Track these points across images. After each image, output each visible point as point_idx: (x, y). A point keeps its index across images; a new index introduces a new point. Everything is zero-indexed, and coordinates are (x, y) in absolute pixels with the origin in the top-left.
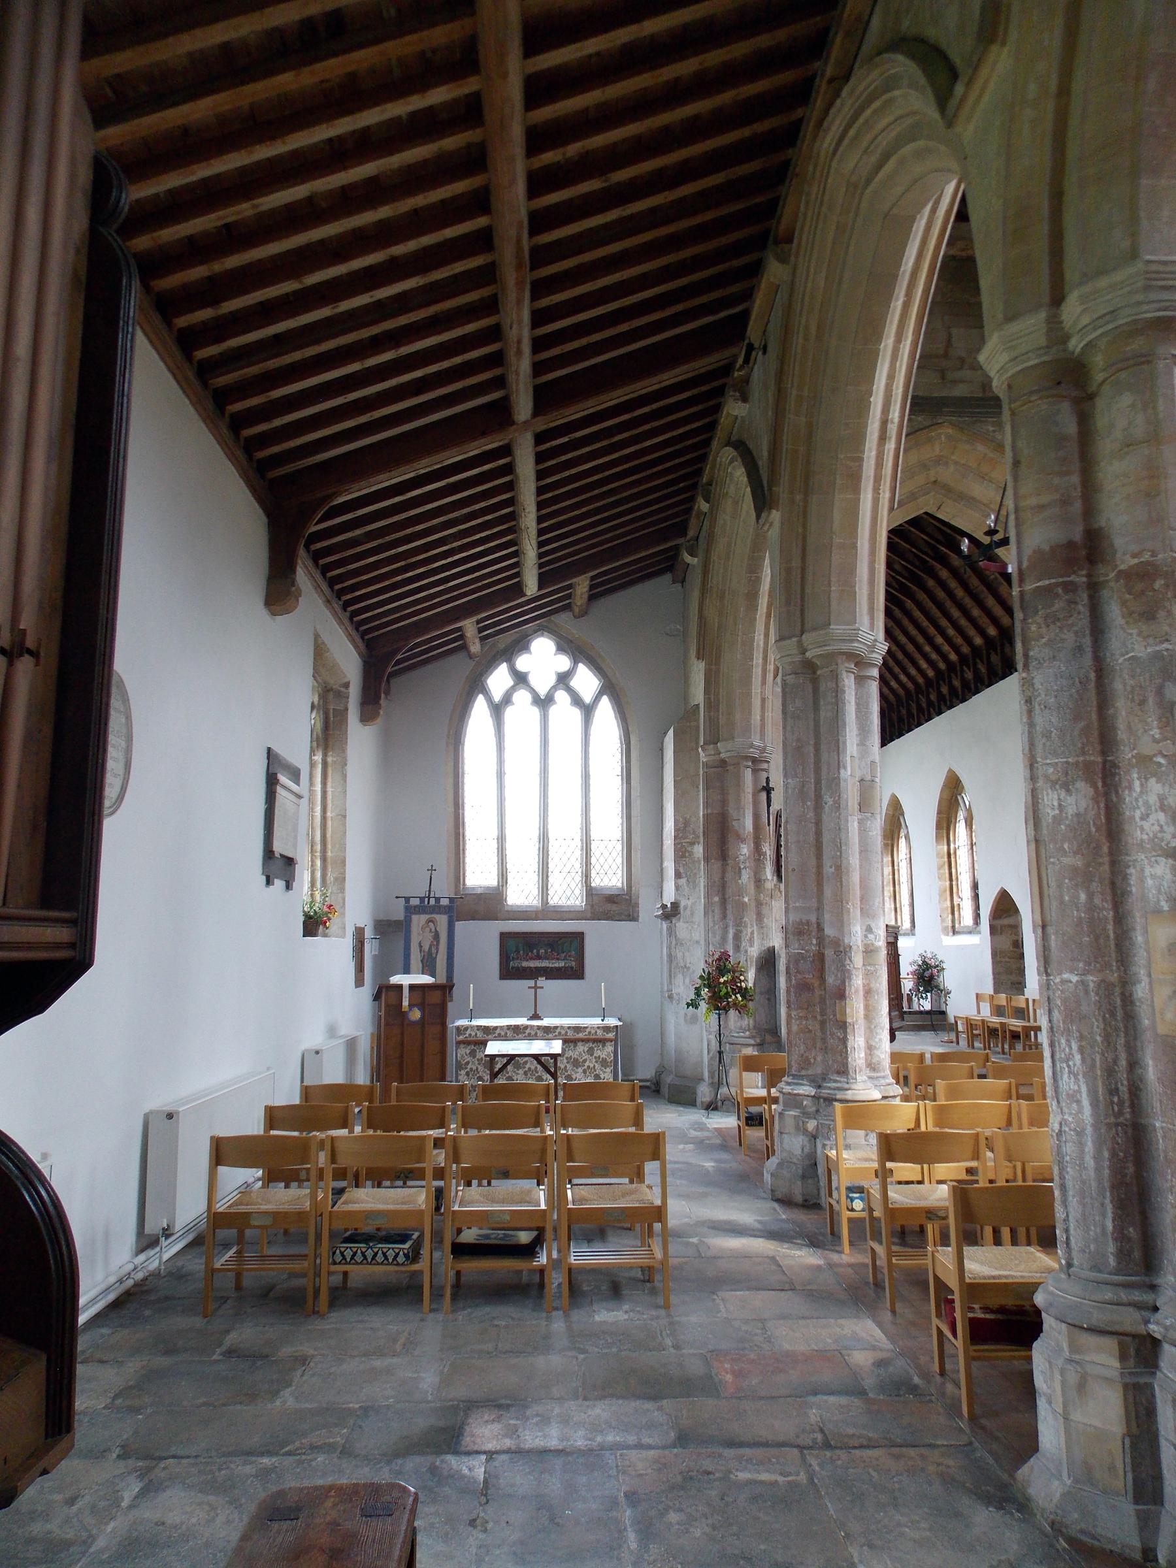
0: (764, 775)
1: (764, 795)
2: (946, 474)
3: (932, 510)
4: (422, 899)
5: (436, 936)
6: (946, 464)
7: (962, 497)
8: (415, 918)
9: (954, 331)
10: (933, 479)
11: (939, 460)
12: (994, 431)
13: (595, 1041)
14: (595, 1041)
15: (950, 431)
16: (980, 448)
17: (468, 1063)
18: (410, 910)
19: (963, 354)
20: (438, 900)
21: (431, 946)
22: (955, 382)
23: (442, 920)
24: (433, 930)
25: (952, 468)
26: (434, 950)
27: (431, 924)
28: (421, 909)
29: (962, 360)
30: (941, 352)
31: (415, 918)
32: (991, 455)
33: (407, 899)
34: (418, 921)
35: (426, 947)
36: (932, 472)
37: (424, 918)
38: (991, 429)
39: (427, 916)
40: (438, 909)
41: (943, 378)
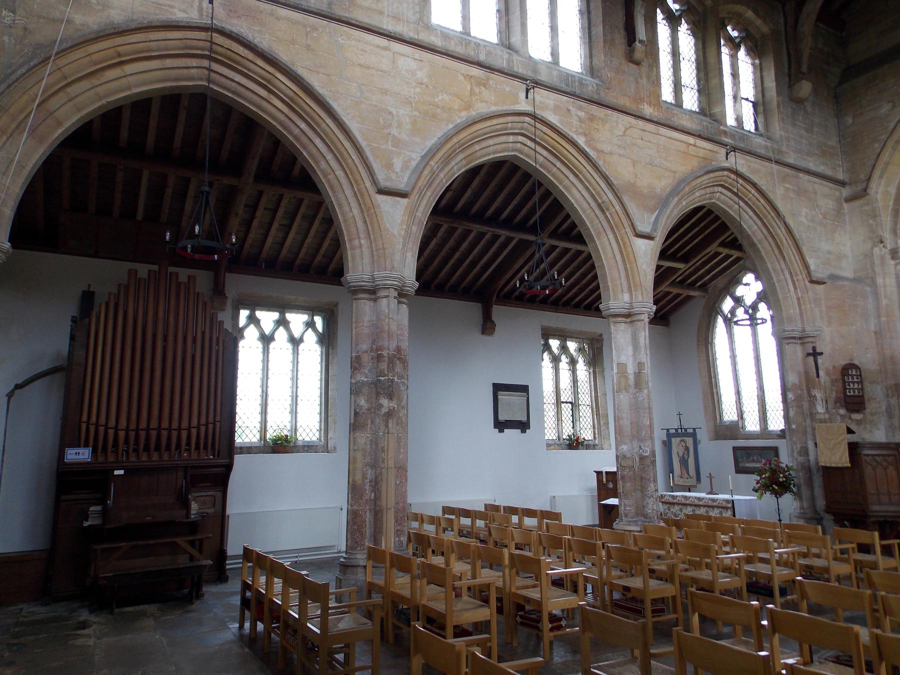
0: (811, 345)
1: (811, 359)
4: (677, 430)
5: (687, 449)
8: (673, 440)
13: (722, 508)
14: (722, 508)
17: (679, 514)
18: (669, 436)
20: (686, 430)
21: (683, 454)
23: (690, 441)
24: (684, 445)
26: (686, 456)
27: (682, 443)
28: (676, 435)
31: (673, 440)
33: (668, 430)
34: (675, 441)
35: (681, 455)
37: (679, 439)
39: (680, 439)
40: (685, 434)
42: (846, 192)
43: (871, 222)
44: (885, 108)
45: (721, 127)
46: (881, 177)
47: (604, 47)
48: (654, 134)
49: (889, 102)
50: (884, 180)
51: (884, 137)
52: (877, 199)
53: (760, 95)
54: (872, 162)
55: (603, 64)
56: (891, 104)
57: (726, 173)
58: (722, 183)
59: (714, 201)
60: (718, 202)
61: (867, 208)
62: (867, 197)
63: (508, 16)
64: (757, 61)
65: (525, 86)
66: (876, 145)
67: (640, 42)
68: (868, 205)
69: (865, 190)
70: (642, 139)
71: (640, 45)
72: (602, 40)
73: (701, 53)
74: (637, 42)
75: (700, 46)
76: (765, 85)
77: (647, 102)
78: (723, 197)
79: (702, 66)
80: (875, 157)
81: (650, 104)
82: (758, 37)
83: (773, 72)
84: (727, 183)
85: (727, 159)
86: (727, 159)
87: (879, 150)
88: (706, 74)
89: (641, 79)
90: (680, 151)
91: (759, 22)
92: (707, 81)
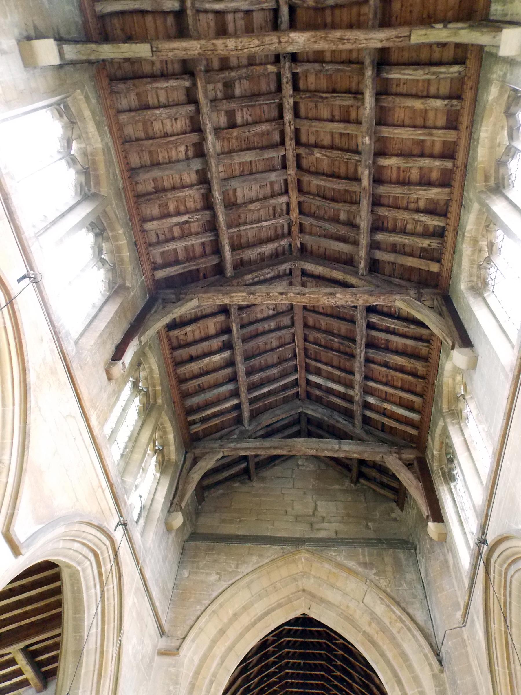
2: (310, 584)
3: (307, 612)
6: (308, 578)
7: (322, 601)
9: (319, 503)
10: (301, 588)
11: (305, 575)
12: (336, 555)
15: (307, 555)
16: (326, 566)
19: (324, 515)
22: (318, 530)
25: (312, 580)
29: (323, 518)
30: (311, 514)
32: (334, 570)
36: (300, 583)
38: (334, 554)
41: (312, 527)
42: (162, 643)
43: (171, 688)
44: (214, 577)
45: (126, 497)
46: (193, 641)
47: (98, 338)
48: (85, 445)
49: (218, 573)
50: (194, 645)
51: (207, 602)
52: (183, 663)
53: (150, 502)
54: (190, 622)
55: (90, 347)
56: (218, 576)
57: (108, 543)
58: (99, 552)
59: (79, 568)
60: (81, 574)
61: (173, 670)
62: (175, 658)
63: (53, 225)
64: (158, 475)
65: (24, 272)
66: (198, 607)
67: (123, 363)
68: (175, 667)
69: (178, 649)
70: (74, 439)
71: (122, 365)
72: (100, 332)
73: (137, 429)
74: (121, 362)
75: (140, 424)
76: (156, 497)
77: (97, 414)
78: (89, 571)
79: (134, 438)
80: (194, 618)
81: (98, 417)
82: (166, 458)
83: (166, 488)
84: (102, 555)
85: (115, 530)
86: (115, 530)
87: (199, 613)
88: (134, 447)
89: (105, 392)
90: (92, 484)
91: (173, 448)
92: (132, 451)
